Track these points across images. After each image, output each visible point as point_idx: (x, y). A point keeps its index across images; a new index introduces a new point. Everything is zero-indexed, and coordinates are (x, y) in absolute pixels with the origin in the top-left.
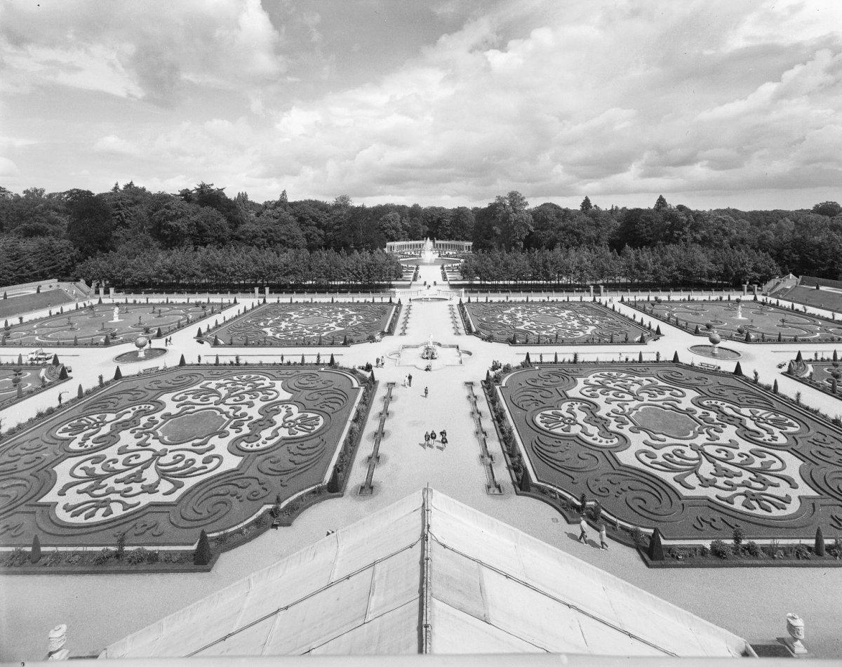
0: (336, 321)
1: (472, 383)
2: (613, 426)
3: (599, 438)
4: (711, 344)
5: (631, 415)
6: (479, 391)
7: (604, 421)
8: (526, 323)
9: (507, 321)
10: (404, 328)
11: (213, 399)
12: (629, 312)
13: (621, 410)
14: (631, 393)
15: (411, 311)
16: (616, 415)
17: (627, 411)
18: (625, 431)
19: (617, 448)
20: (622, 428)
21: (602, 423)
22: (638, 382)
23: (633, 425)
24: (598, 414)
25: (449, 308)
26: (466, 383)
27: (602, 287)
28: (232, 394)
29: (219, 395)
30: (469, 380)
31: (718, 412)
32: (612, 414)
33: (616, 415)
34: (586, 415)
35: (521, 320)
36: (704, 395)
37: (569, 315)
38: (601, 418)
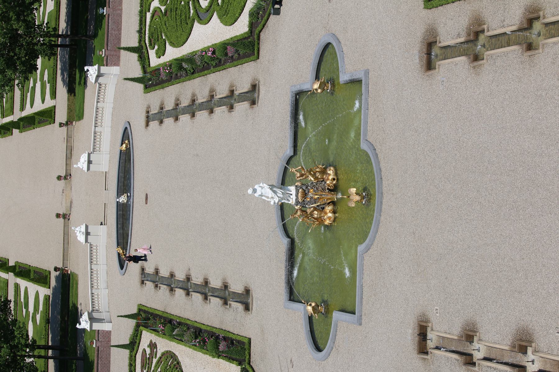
1: (430, 46)
25: (154, 124)
26: (429, 66)
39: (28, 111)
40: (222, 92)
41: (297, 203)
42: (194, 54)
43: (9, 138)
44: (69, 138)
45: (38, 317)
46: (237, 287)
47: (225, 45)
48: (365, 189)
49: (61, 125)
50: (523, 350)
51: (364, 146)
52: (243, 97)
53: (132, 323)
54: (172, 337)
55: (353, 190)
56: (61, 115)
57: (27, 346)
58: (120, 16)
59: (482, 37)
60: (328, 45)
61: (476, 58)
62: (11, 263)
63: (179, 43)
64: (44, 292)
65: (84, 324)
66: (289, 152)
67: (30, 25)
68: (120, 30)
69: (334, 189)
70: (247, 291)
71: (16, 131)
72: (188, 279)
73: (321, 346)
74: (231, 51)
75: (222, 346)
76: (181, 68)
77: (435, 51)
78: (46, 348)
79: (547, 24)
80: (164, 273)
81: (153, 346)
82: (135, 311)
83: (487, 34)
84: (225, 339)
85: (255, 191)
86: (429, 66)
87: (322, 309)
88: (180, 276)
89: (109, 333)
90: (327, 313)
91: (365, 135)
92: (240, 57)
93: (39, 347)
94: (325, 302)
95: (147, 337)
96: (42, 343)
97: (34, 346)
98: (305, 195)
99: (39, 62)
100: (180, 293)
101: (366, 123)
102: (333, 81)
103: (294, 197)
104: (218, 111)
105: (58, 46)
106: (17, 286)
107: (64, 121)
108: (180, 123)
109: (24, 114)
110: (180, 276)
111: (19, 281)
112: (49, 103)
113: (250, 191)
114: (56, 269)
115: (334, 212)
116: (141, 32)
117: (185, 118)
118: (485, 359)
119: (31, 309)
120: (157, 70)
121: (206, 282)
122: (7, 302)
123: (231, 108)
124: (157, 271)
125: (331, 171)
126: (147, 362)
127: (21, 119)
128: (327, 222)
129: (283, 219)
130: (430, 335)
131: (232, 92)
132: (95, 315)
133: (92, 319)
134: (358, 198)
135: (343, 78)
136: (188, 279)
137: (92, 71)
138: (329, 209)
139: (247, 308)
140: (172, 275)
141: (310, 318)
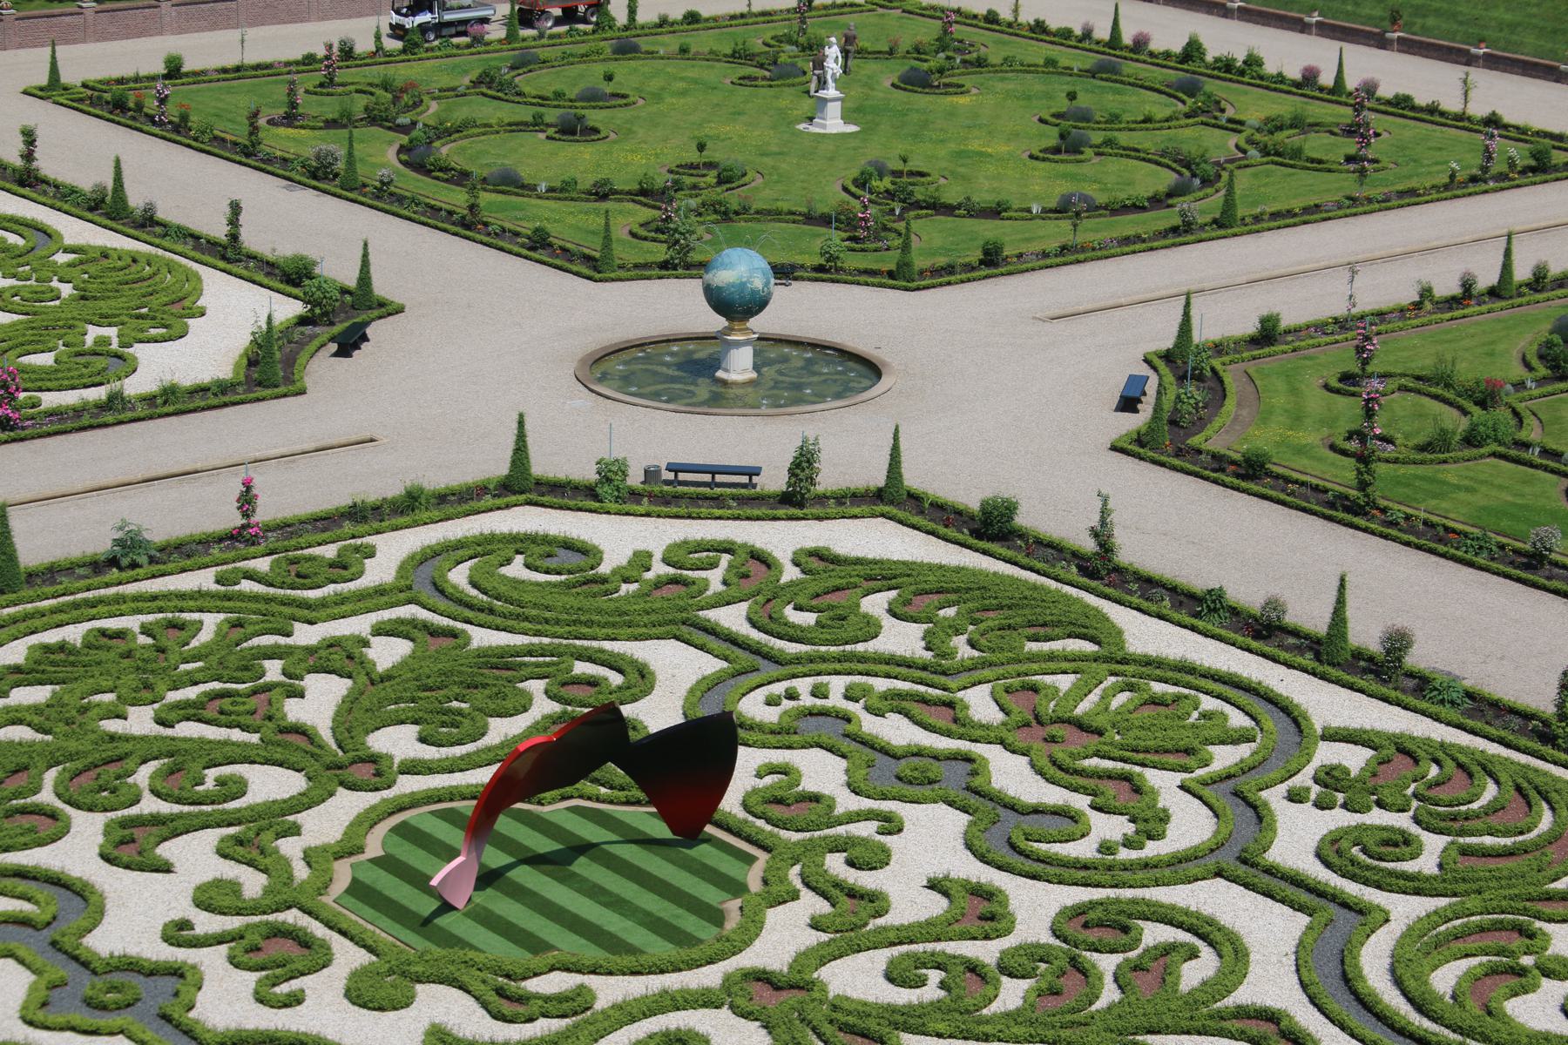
4: (718, 322)
5: (328, 900)
7: (156, 993)
13: (253, 883)
16: (233, 923)
17: (301, 872)
20: (295, 1000)
23: (361, 957)
24: (104, 941)
31: (846, 745)
32: (206, 923)
33: (233, 923)
34: (26, 978)
36: (745, 658)
38: (131, 966)
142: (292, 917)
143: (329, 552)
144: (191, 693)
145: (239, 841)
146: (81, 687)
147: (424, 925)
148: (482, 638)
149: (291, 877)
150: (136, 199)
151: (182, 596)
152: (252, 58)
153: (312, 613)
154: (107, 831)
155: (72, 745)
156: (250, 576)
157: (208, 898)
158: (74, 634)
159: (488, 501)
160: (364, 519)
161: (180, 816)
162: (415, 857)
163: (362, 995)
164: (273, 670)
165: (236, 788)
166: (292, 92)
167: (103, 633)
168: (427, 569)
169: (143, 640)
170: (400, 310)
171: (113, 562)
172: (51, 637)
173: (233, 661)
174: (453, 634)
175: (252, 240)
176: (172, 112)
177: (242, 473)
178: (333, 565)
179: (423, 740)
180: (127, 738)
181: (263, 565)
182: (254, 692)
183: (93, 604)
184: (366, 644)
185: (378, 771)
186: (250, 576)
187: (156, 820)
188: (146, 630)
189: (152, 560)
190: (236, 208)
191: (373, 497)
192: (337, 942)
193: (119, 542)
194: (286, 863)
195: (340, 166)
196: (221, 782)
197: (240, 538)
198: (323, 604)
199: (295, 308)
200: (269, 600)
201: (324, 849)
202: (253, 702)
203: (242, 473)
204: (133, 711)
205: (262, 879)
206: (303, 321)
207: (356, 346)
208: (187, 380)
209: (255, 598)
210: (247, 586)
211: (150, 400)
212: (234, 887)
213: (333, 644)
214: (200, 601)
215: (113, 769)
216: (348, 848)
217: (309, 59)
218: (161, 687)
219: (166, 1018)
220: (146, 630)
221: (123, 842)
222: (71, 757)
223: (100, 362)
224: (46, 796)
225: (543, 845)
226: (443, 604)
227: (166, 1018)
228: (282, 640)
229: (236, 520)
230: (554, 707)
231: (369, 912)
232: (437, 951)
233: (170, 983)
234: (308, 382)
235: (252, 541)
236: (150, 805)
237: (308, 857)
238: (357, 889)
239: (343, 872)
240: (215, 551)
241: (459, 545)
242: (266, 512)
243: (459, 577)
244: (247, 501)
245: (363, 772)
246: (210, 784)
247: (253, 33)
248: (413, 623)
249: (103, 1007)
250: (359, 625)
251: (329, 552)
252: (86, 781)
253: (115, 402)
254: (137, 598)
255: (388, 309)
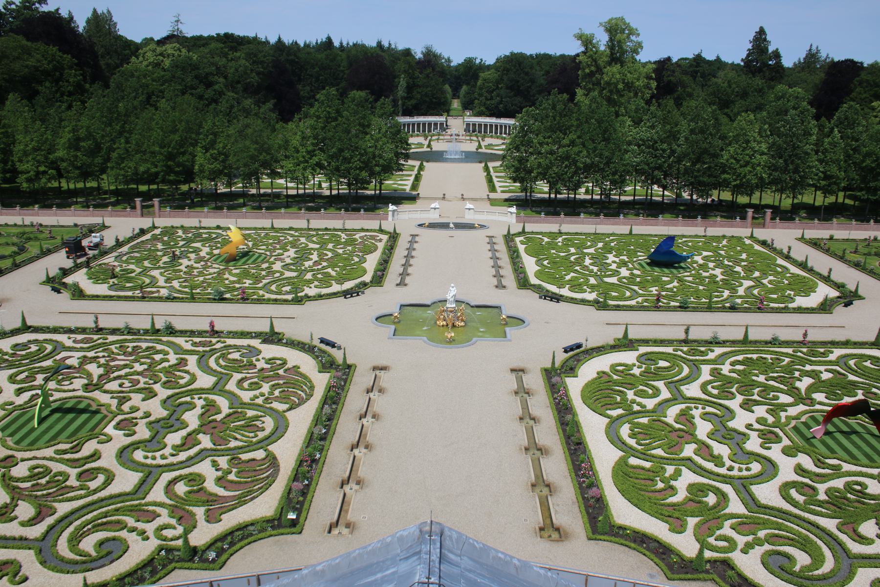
0: (282, 260)
1: (522, 370)
2: (753, 444)
3: (728, 463)
5: (787, 428)
6: (535, 381)
7: (738, 438)
8: (624, 272)
9: (591, 267)
10: (404, 274)
11: (78, 383)
12: (801, 252)
13: (771, 419)
14: (793, 391)
15: (415, 246)
16: (762, 427)
17: (783, 420)
18: (775, 453)
19: (760, 478)
20: (769, 448)
21: (734, 438)
22: (814, 374)
24: (731, 424)
25: (487, 240)
26: (513, 370)
27: (769, 212)
28: (112, 376)
29: (89, 375)
30: (515, 365)
32: (756, 426)
33: (762, 427)
35: (614, 266)
37: (705, 258)
38: (735, 431)
39: (495, 180)
40: (502, 272)
41: (447, 308)
42: (521, 259)
43: (482, 170)
44: (482, 199)
45: (396, 186)
46: (408, 280)
47: (525, 273)
48: (454, 340)
49: (488, 195)
50: (374, 417)
51: (474, 339)
52: (500, 282)
53: (392, 231)
54: (385, 249)
55: (453, 335)
56: (493, 196)
57: (381, 180)
58: (540, 223)
59: (526, 395)
60: (524, 322)
61: (516, 393)
62: (422, 173)
63: (526, 250)
64: (408, 189)
65: (392, 207)
66: (472, 304)
67: (536, 179)
68: (533, 223)
69: (454, 326)
70: (406, 285)
71: (486, 174)
72: (412, 257)
73: (379, 320)
74: (522, 276)
75: (379, 273)
76: (514, 252)
77: (520, 373)
78: (380, 190)
79: (532, 427)
80: (415, 246)
81: (380, 240)
82: (397, 232)
83: (528, 398)
84: (383, 274)
85: (453, 287)
86: (513, 370)
87: (396, 320)
88: (414, 253)
89: (387, 219)
90: (394, 323)
91: (480, 340)
92: (519, 280)
93: (380, 187)
94: (399, 322)
95: (385, 238)
96: (383, 187)
97: (381, 184)
98: (451, 312)
99: (518, 184)
100: (406, 253)
101: (486, 340)
102: (506, 324)
103: (450, 306)
104: (493, 270)
105: (526, 193)
106: (410, 175)
107: (490, 197)
108: (488, 252)
109: (494, 178)
110: (414, 253)
111: (413, 176)
112: (499, 190)
113: (452, 285)
114: (418, 194)
115: (443, 326)
116: (533, 233)
117: (490, 254)
118: (370, 399)
119: (399, 182)
120: (513, 240)
121: (410, 265)
122: (402, 170)
123: (495, 276)
124: (416, 242)
125: (462, 324)
126: (373, 237)
127: (491, 176)
128: (438, 322)
129: (440, 301)
130: (382, 372)
131: (502, 277)
132: (396, 213)
133: (394, 211)
134: (449, 337)
135: (508, 329)
136: (412, 257)
137: (514, 209)
138: (445, 323)
139: (397, 285)
140: (414, 249)
141: (391, 315)
142: (777, 430)
143: (822, 350)
144: (775, 375)
145: (771, 410)
146: (751, 368)
147: (807, 440)
148: (851, 377)
149: (780, 421)
150: (810, 264)
151: (783, 353)
152: (851, 237)
153: (812, 363)
154: (744, 400)
155: (744, 380)
156: (801, 352)
157: (758, 421)
158: (755, 356)
159: (867, 346)
160: (834, 345)
161: (761, 401)
162: (811, 423)
163: (787, 452)
164: (797, 374)
165: (777, 398)
166: (857, 246)
167: (761, 357)
168: (845, 359)
169: (770, 361)
170: (864, 299)
171: (770, 343)
172: (749, 356)
173: (788, 370)
174: (844, 375)
175: (833, 277)
176: (827, 247)
177: (805, 328)
178: (822, 353)
179: (826, 398)
180: (756, 381)
181: (805, 350)
182: (790, 378)
183: (761, 351)
184: (822, 373)
185: (812, 402)
186: (801, 352)
187: (755, 401)
188: (771, 359)
189: (780, 344)
190: (831, 270)
191: (837, 340)
192: (784, 437)
193: (773, 338)
194: (781, 417)
195: (862, 264)
196: (773, 396)
197: (802, 343)
198: (815, 362)
199: (836, 294)
200: (803, 358)
201: (790, 416)
202: (788, 380)
203: (805, 328)
204: (760, 376)
205: (773, 419)
206: (839, 297)
207: (849, 305)
208: (804, 306)
209: (800, 357)
210: (799, 354)
211: (794, 309)
212: (766, 420)
213: (813, 371)
214: (787, 355)
215: (751, 387)
216: (796, 418)
217: (866, 239)
218: (769, 372)
219: (738, 444)
220: (771, 359)
221: (745, 404)
222: (742, 383)
223: (787, 299)
224: (734, 390)
225: (845, 429)
226: (844, 367)
227: (738, 444)
228: (801, 367)
229: (801, 339)
230: (863, 398)
231: (795, 433)
232: (807, 446)
233: (742, 437)
234: (834, 311)
235: (805, 344)
236: (756, 397)
237: (787, 417)
238: (795, 428)
239: (793, 423)
240: (795, 345)
241: (855, 355)
242: (809, 339)
243: (852, 363)
244: (805, 335)
245: (809, 401)
246: (771, 396)
247: (852, 232)
248: (835, 371)
249: (725, 438)
250: (822, 368)
251: (822, 350)
252: (743, 388)
253: (786, 308)
254: (772, 351)
255: (861, 298)
